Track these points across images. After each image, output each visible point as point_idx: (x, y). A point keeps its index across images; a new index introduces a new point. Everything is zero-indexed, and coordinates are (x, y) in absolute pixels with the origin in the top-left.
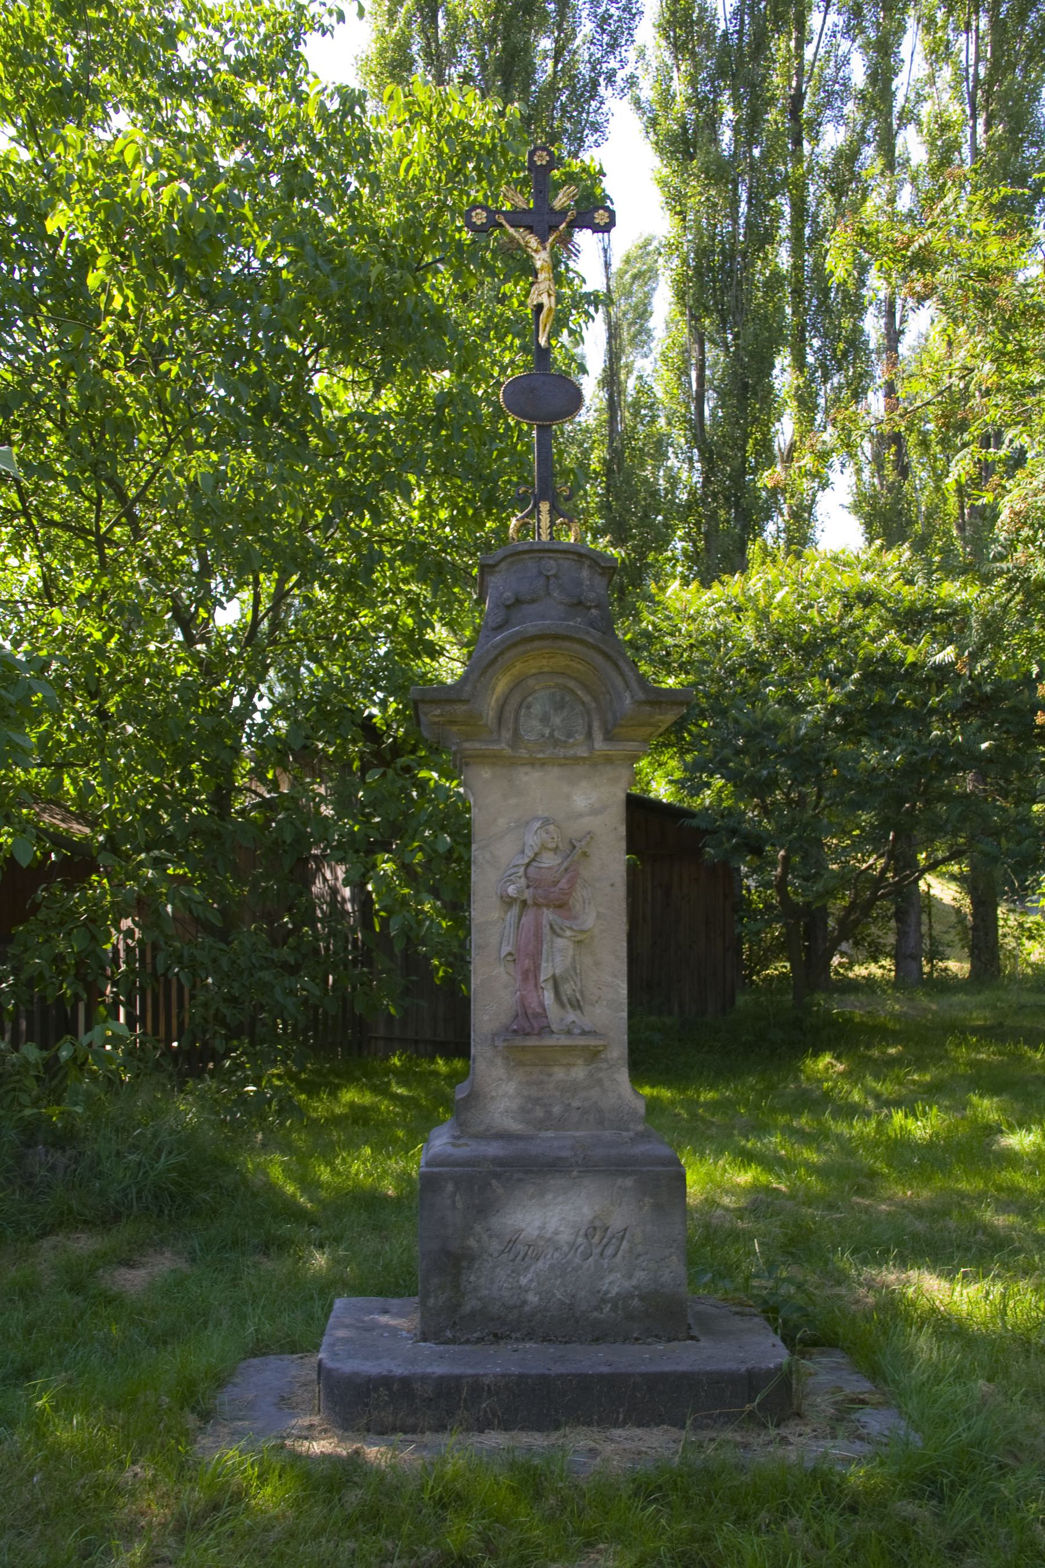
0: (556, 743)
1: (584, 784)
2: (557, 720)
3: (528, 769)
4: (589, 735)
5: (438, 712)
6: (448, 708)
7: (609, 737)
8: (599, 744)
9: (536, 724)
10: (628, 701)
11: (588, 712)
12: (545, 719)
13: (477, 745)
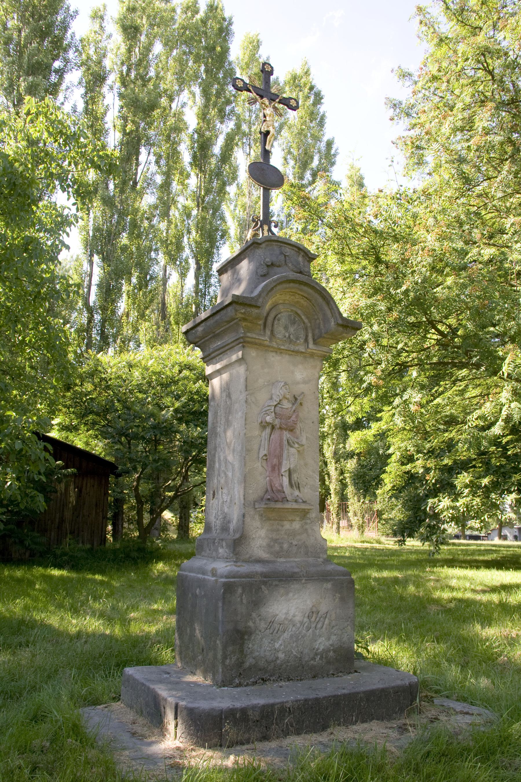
0: (291, 342)
1: (300, 366)
2: (292, 330)
3: (274, 354)
4: (306, 340)
5: (243, 311)
6: (248, 309)
7: (315, 342)
8: (311, 345)
9: (281, 329)
10: (333, 323)
11: (306, 329)
12: (286, 328)
13: (254, 336)
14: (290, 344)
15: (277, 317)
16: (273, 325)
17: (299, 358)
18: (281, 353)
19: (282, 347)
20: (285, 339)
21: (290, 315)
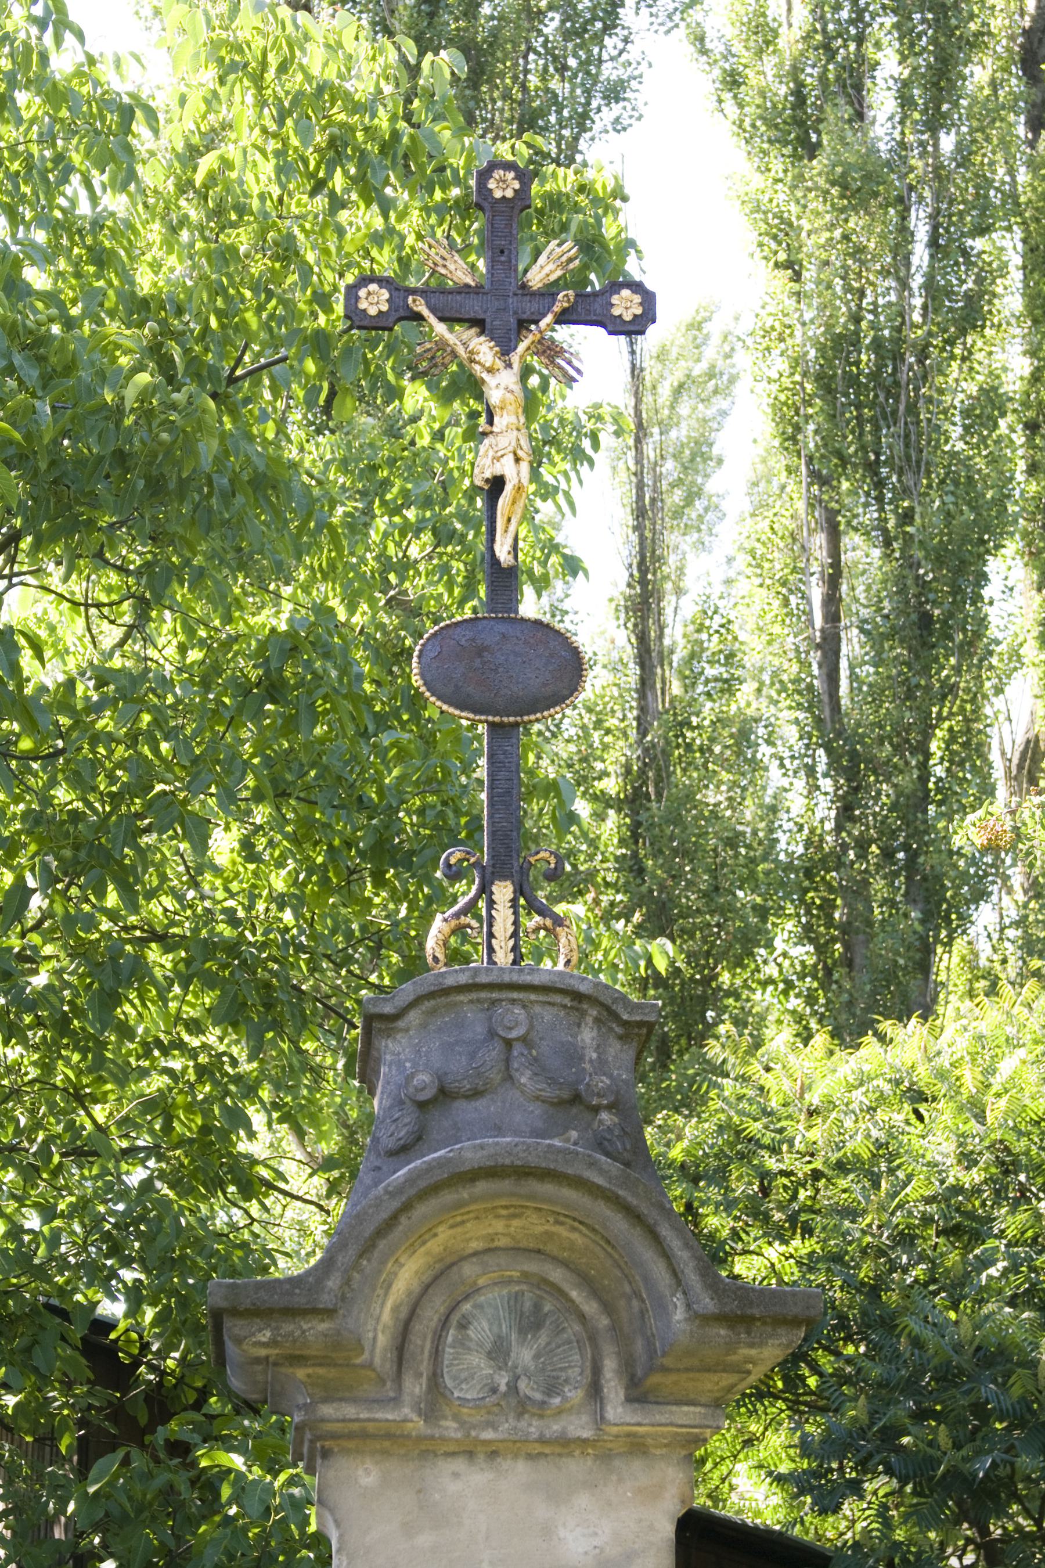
0: (523, 1406)
1: (583, 1500)
2: (524, 1356)
3: (459, 1465)
4: (595, 1391)
5: (266, 1336)
6: (287, 1327)
7: (638, 1394)
8: (616, 1409)
9: (477, 1360)
10: (679, 1315)
11: (593, 1338)
12: (498, 1353)
13: (350, 1411)
14: (520, 1416)
15: (455, 1318)
16: (437, 1354)
17: (576, 1467)
18: (493, 1455)
19: (488, 1435)
20: (494, 1399)
21: (517, 1296)
